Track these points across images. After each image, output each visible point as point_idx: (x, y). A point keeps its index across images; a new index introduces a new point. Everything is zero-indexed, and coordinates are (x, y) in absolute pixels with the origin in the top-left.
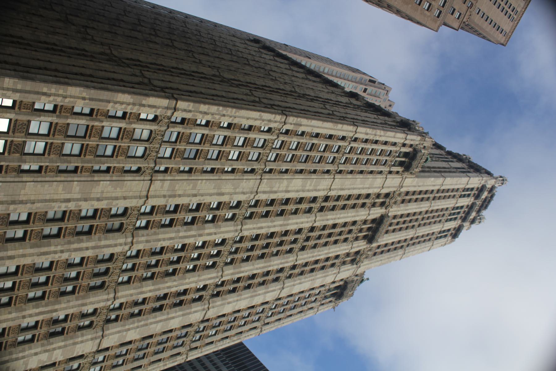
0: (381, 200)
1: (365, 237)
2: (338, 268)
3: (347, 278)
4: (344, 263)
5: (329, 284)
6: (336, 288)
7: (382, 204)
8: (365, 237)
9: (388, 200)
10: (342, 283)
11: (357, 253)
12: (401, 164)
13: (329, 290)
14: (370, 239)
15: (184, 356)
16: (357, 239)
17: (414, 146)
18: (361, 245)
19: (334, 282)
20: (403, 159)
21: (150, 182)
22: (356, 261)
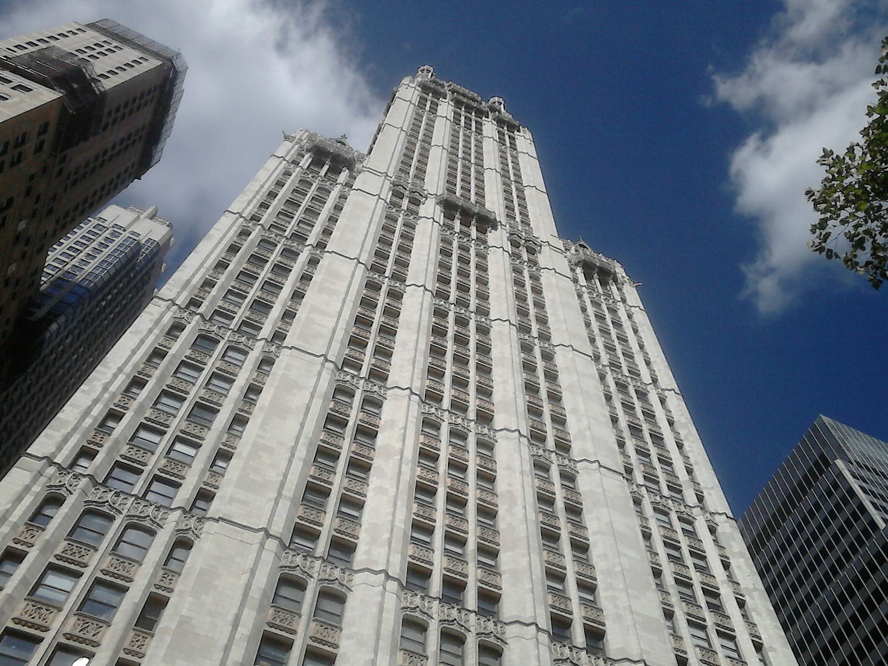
0: (405, 203)
1: (482, 230)
2: (542, 270)
3: (570, 262)
4: (533, 263)
5: (576, 286)
6: (588, 277)
7: (415, 202)
8: (482, 230)
9: (407, 193)
10: (579, 270)
11: (515, 244)
12: (335, 170)
13: (592, 289)
14: (486, 222)
15: (718, 519)
16: (482, 241)
17: (303, 152)
18: (497, 238)
19: (575, 281)
20: (326, 167)
21: (220, 522)
22: (533, 246)
